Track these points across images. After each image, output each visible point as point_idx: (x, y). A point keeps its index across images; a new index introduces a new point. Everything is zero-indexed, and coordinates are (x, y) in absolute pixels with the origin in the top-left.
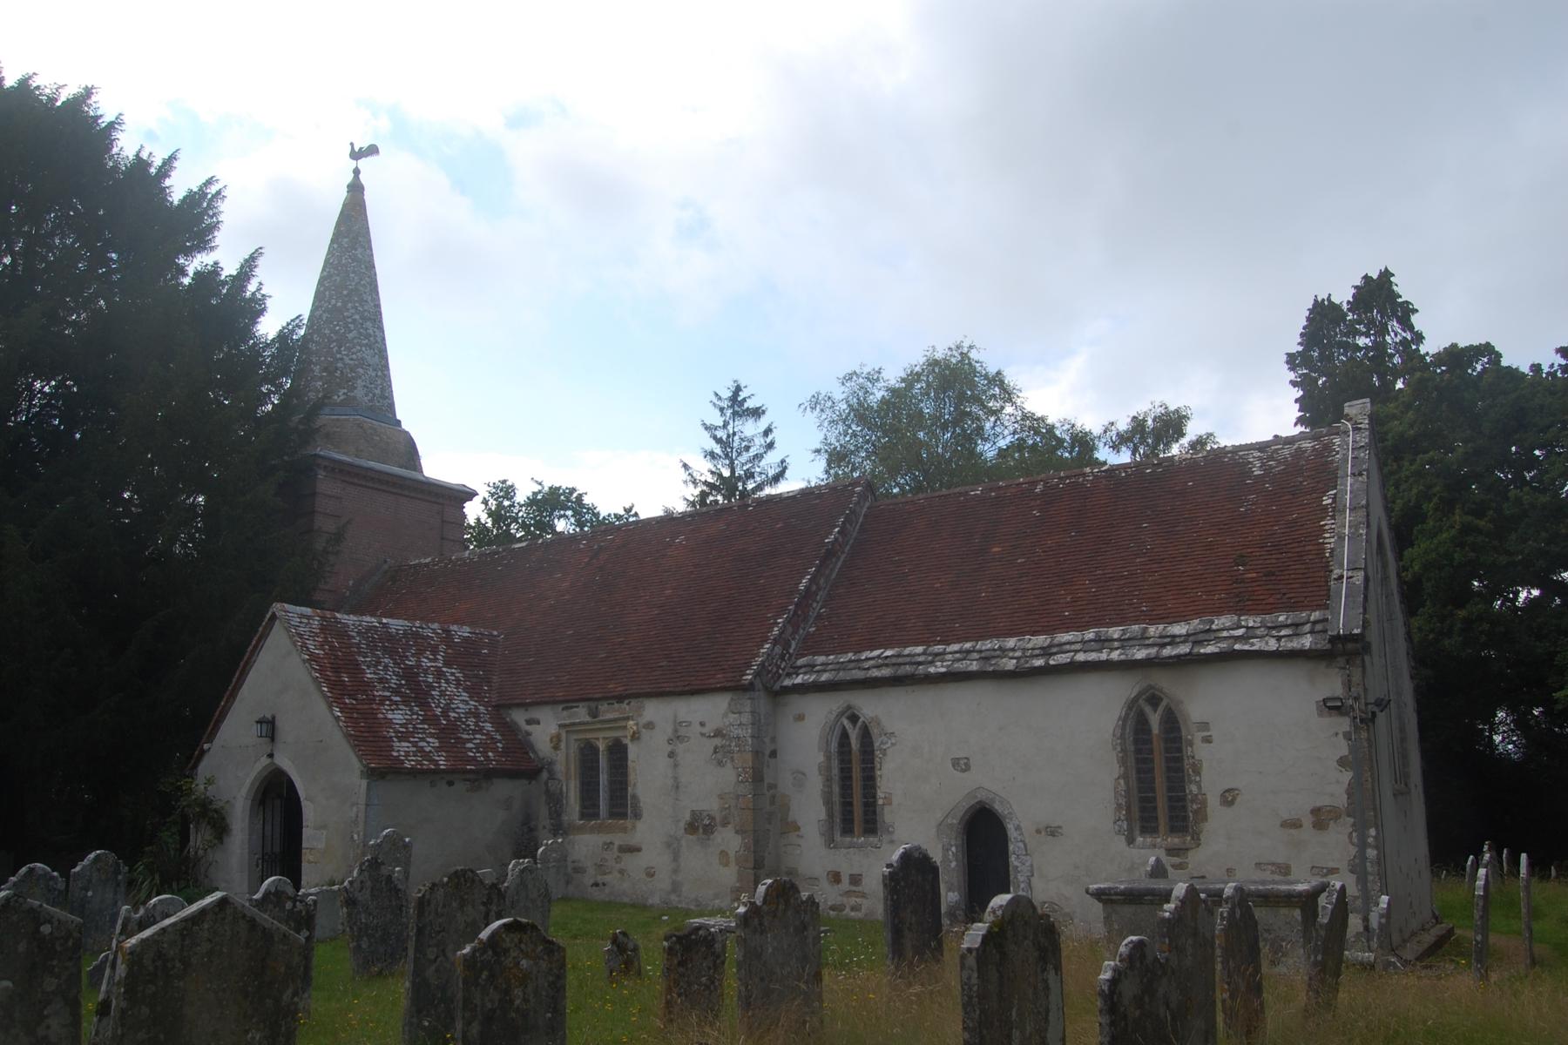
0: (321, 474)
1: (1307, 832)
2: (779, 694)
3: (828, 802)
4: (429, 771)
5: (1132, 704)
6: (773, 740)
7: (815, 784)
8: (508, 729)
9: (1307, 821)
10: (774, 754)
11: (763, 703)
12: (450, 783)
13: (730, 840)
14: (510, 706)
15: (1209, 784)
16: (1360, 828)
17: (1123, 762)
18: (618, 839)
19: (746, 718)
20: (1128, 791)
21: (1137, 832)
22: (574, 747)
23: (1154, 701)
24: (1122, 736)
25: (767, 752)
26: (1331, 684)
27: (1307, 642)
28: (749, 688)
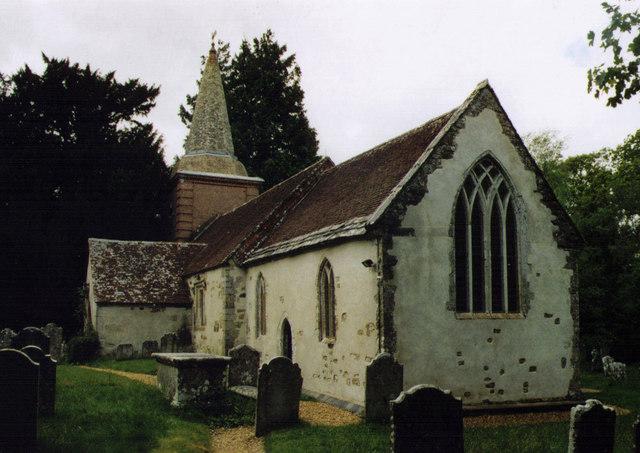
0: (182, 181)
1: (365, 336)
2: (245, 268)
3: (257, 318)
4: (127, 303)
5: (322, 269)
6: (244, 289)
7: (254, 308)
8: (184, 285)
9: (365, 332)
10: (244, 295)
11: (235, 273)
12: (141, 309)
13: (221, 334)
14: (189, 276)
15: (338, 313)
16: (379, 335)
17: (320, 300)
18: (204, 333)
19: (224, 279)
20: (320, 314)
21: (324, 335)
22: (199, 293)
23: (329, 265)
24: (319, 286)
25: (237, 295)
26: (371, 251)
27: (358, 232)
28: (226, 265)
